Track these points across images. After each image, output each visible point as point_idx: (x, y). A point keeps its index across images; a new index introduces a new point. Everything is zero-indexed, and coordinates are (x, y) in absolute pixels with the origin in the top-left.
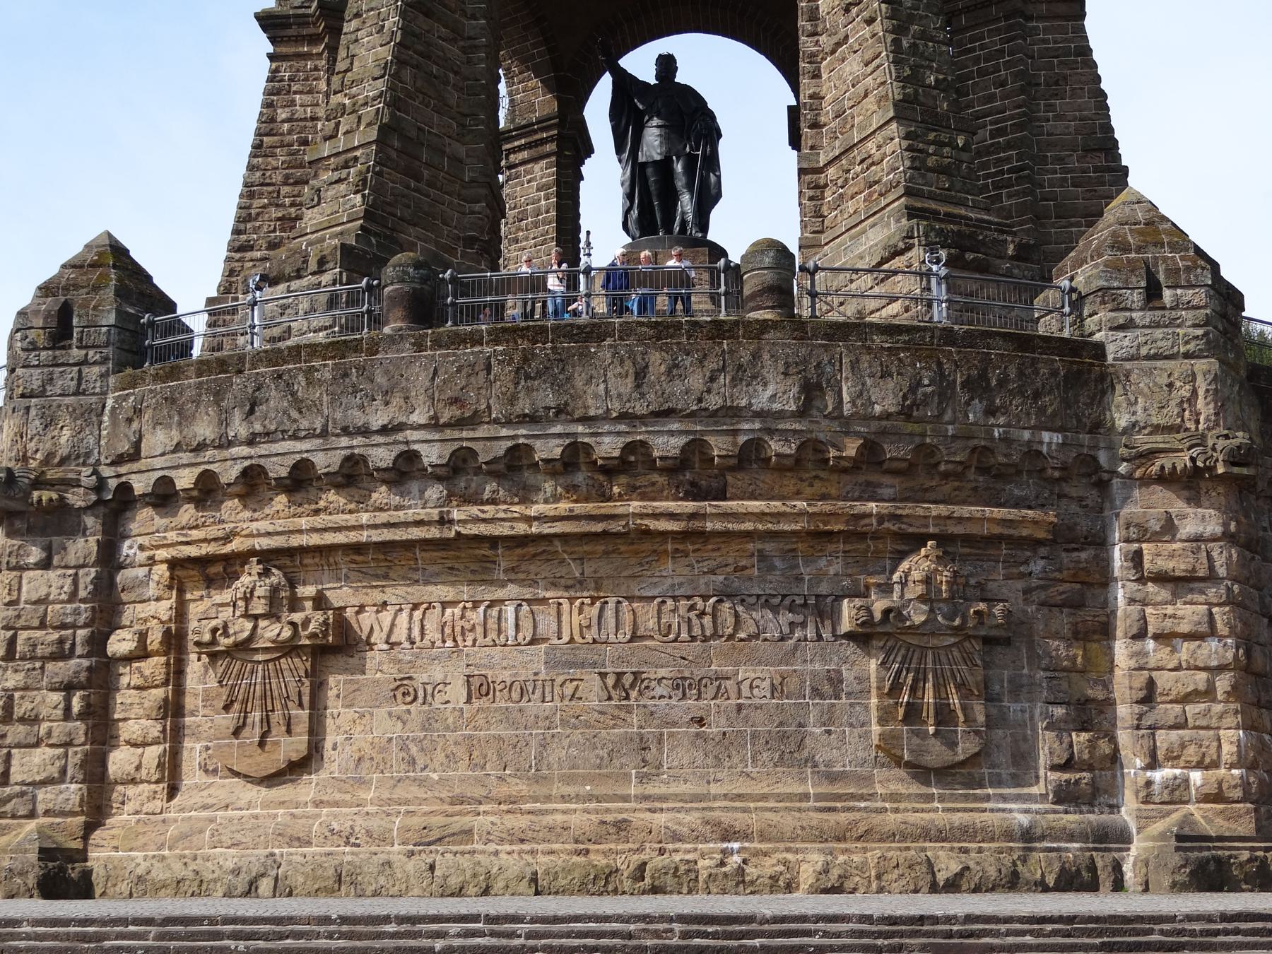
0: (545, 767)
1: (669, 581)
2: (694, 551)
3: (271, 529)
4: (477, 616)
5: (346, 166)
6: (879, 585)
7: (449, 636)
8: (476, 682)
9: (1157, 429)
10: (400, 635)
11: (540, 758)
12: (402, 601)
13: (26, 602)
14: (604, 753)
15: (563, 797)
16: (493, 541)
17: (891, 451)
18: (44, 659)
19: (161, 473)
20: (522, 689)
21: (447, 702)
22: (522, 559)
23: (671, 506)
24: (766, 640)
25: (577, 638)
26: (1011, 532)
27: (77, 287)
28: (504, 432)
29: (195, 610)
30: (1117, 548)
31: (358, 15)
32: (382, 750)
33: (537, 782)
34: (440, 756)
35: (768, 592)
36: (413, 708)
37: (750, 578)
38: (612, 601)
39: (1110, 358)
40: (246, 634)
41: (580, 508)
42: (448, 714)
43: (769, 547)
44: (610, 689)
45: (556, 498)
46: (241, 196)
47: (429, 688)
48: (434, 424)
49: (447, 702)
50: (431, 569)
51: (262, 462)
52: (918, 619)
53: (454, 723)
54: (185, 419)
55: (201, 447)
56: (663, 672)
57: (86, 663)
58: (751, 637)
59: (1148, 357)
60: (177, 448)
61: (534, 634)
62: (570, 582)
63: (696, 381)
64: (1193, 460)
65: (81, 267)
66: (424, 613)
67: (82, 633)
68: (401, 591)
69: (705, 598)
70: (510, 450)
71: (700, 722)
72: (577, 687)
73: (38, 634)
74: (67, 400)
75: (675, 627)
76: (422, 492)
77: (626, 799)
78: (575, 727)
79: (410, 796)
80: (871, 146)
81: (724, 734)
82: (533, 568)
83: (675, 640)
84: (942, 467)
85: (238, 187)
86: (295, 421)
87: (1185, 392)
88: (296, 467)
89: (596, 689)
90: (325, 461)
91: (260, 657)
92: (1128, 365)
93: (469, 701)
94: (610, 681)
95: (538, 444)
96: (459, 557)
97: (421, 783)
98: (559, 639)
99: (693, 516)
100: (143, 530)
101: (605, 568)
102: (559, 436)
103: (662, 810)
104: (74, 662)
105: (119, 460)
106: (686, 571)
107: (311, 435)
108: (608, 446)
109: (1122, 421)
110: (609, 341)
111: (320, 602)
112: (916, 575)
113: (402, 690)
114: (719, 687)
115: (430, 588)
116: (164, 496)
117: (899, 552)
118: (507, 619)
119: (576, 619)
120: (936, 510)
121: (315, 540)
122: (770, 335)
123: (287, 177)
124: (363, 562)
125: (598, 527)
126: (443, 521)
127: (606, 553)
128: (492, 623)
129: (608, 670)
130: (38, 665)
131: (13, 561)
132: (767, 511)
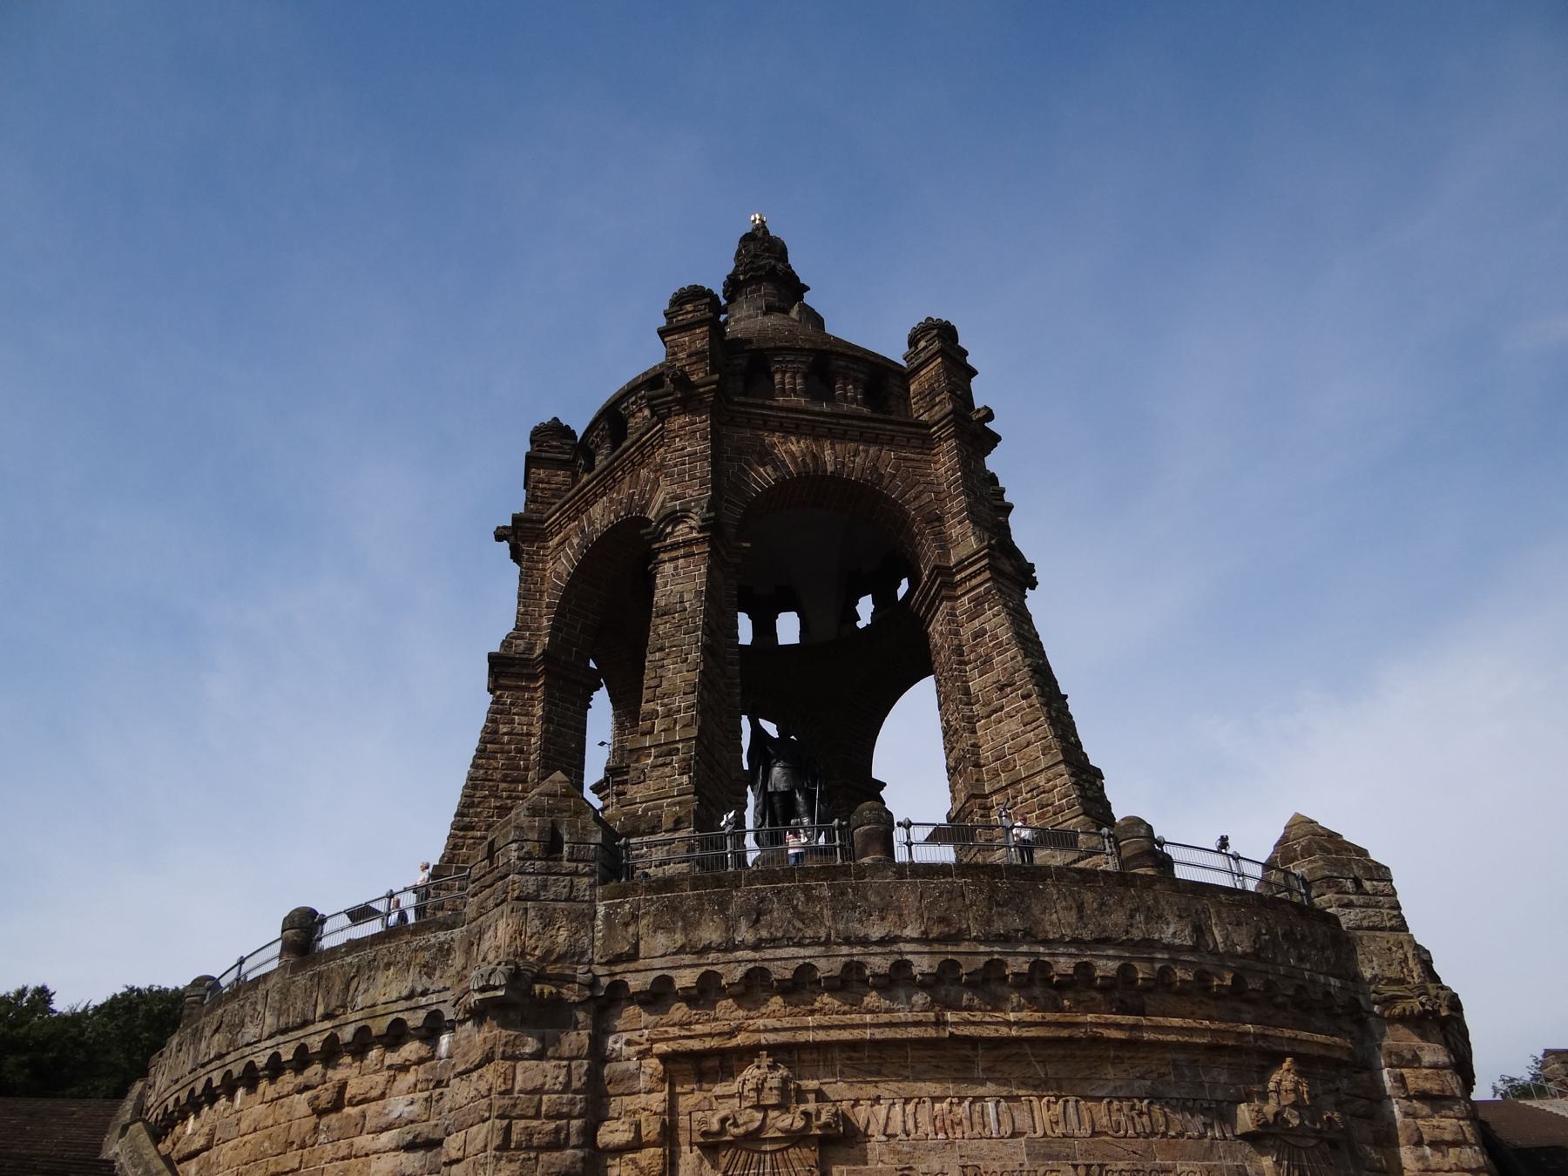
3: (778, 1025)
4: (962, 1111)
5: (670, 753)
6: (1258, 1093)
9: (1391, 981)
10: (896, 1126)
13: (521, 1092)
17: (1254, 984)
18: (541, 1149)
19: (660, 973)
25: (1049, 1132)
26: (1329, 1054)
27: (561, 811)
28: (982, 949)
29: (684, 1103)
30: (1385, 1072)
31: (661, 649)
38: (1071, 1104)
39: (1344, 927)
40: (757, 1124)
41: (1037, 1016)
43: (1181, 1056)
45: (1020, 1008)
46: (466, 787)
48: (924, 939)
51: (766, 964)
52: (1295, 1122)
54: (690, 925)
55: (707, 949)
56: (1121, 1165)
57: (580, 1153)
58: (1180, 1135)
59: (1369, 928)
60: (681, 950)
63: (1119, 917)
64: (1422, 1004)
65: (555, 796)
67: (576, 1123)
68: (893, 1086)
70: (987, 963)
73: (535, 1123)
74: (561, 905)
76: (909, 998)
80: (1040, 780)
84: (1280, 999)
85: (462, 780)
86: (800, 930)
87: (1400, 954)
88: (799, 971)
90: (826, 967)
91: (768, 1148)
92: (1359, 933)
95: (1010, 960)
100: (628, 1026)
102: (1023, 954)
104: (569, 1152)
105: (618, 959)
106: (1123, 1075)
107: (816, 942)
108: (1064, 965)
109: (1368, 974)
110: (1049, 881)
111: (821, 1096)
112: (1287, 1084)
115: (920, 1084)
116: (659, 996)
117: (1262, 1066)
120: (1288, 1033)
121: (821, 1036)
122: (1158, 887)
123: (505, 776)
125: (1065, 1033)
126: (940, 1023)
128: (976, 1116)
130: (532, 1155)
131: (509, 1050)
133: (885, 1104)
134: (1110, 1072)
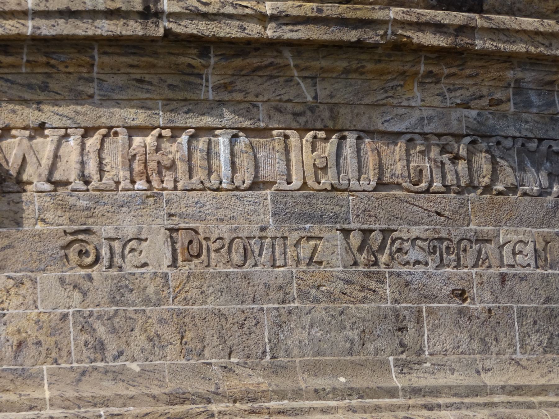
0: (282, 353)
1: (417, 114)
2: (448, 76)
4: (177, 149)
7: (140, 174)
8: (182, 238)
10: (69, 169)
11: (275, 342)
12: (68, 123)
14: (354, 334)
15: (316, 391)
16: (202, 45)
20: (245, 249)
21: (145, 265)
22: (239, 73)
23: (429, 14)
24: (525, 194)
25: (311, 183)
32: (53, 331)
33: (275, 372)
34: (139, 339)
35: (524, 133)
36: (95, 272)
37: (505, 116)
42: (147, 282)
43: (529, 76)
44: (355, 250)
47: (117, 245)
49: (145, 265)
50: (111, 80)
53: (157, 293)
56: (416, 231)
58: (512, 189)
61: (256, 176)
62: (299, 109)
66: (102, 142)
68: (67, 110)
69: (458, 137)
71: (461, 294)
72: (315, 248)
75: (426, 173)
77: (392, 393)
78: (316, 300)
79: (108, 393)
81: (490, 310)
82: (251, 86)
83: (427, 191)
89: (339, 250)
93: (174, 264)
94: (355, 240)
96: (154, 66)
97: (117, 375)
98: (289, 183)
99: (462, 29)
101: (343, 92)
103: (439, 406)
113: (77, 246)
114: (480, 252)
118: (218, 154)
119: (308, 157)
124: (13, 66)
125: (352, 35)
127: (346, 71)
128: (198, 157)
129: (353, 226)
132: (541, 29)
133: (52, 136)
134: (416, 95)
